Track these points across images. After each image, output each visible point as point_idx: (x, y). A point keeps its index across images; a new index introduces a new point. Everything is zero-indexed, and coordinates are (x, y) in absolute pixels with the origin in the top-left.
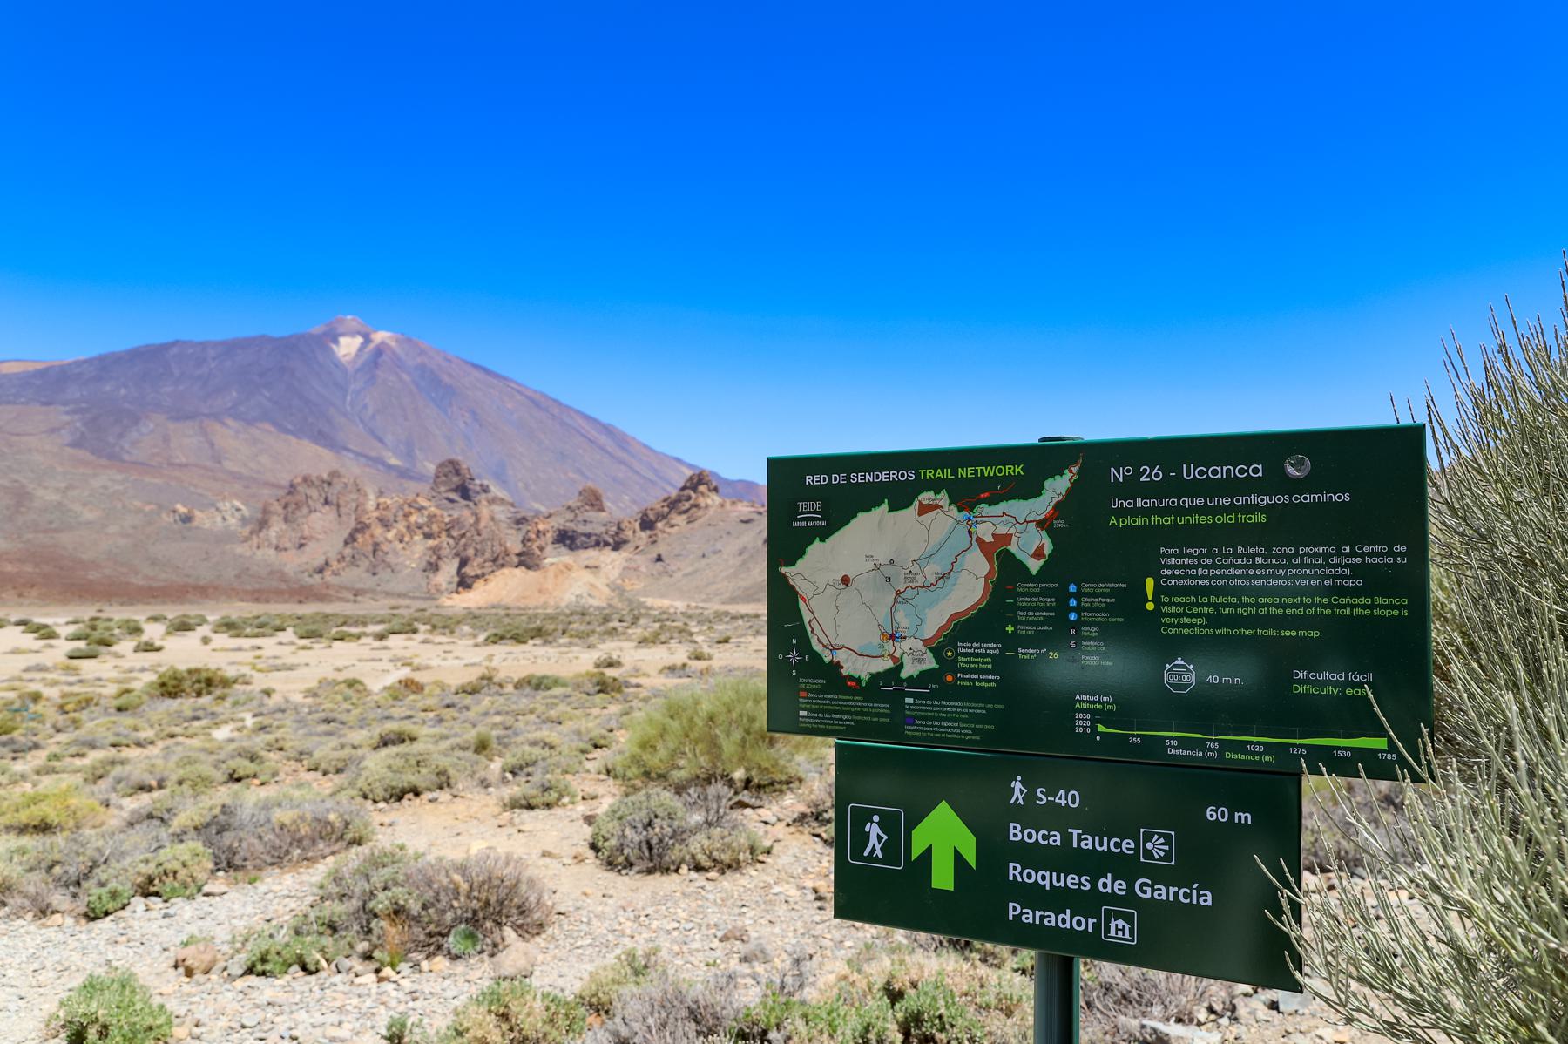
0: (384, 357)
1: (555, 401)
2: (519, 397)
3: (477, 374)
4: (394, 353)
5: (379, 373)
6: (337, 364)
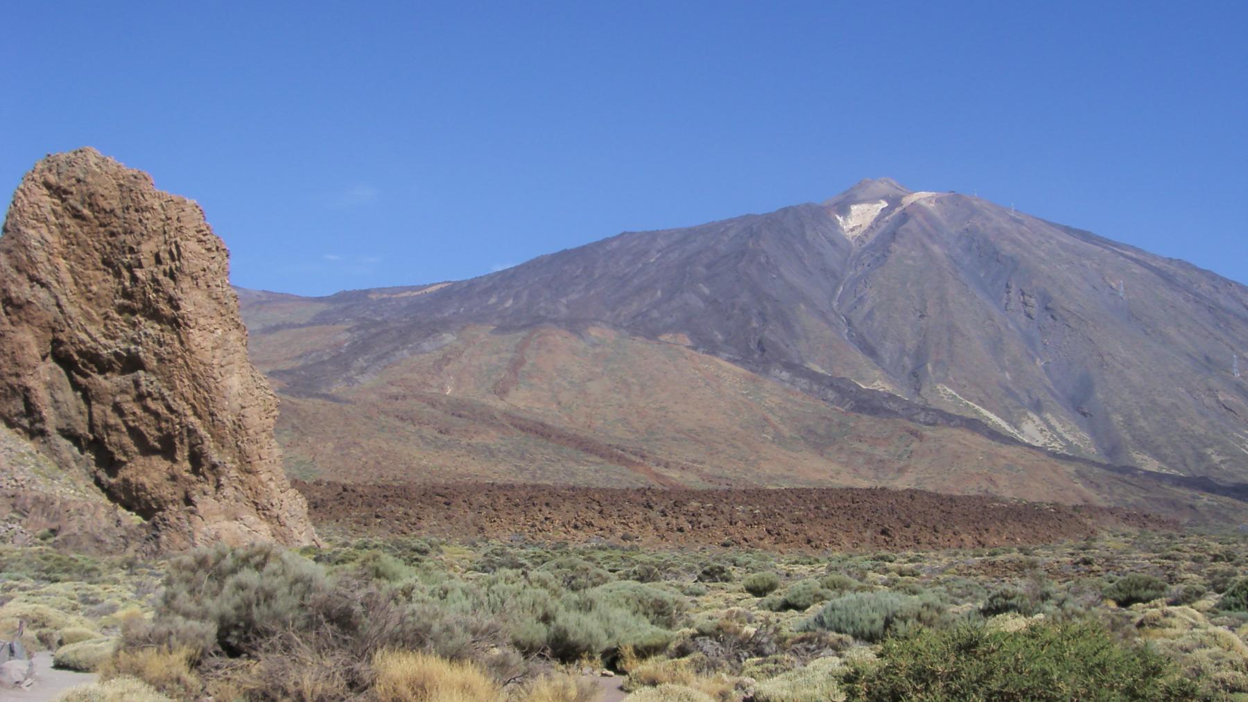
0: (911, 224)
1: (1201, 271)
2: (1137, 269)
3: (1066, 239)
4: (928, 216)
5: (894, 246)
6: (836, 241)
